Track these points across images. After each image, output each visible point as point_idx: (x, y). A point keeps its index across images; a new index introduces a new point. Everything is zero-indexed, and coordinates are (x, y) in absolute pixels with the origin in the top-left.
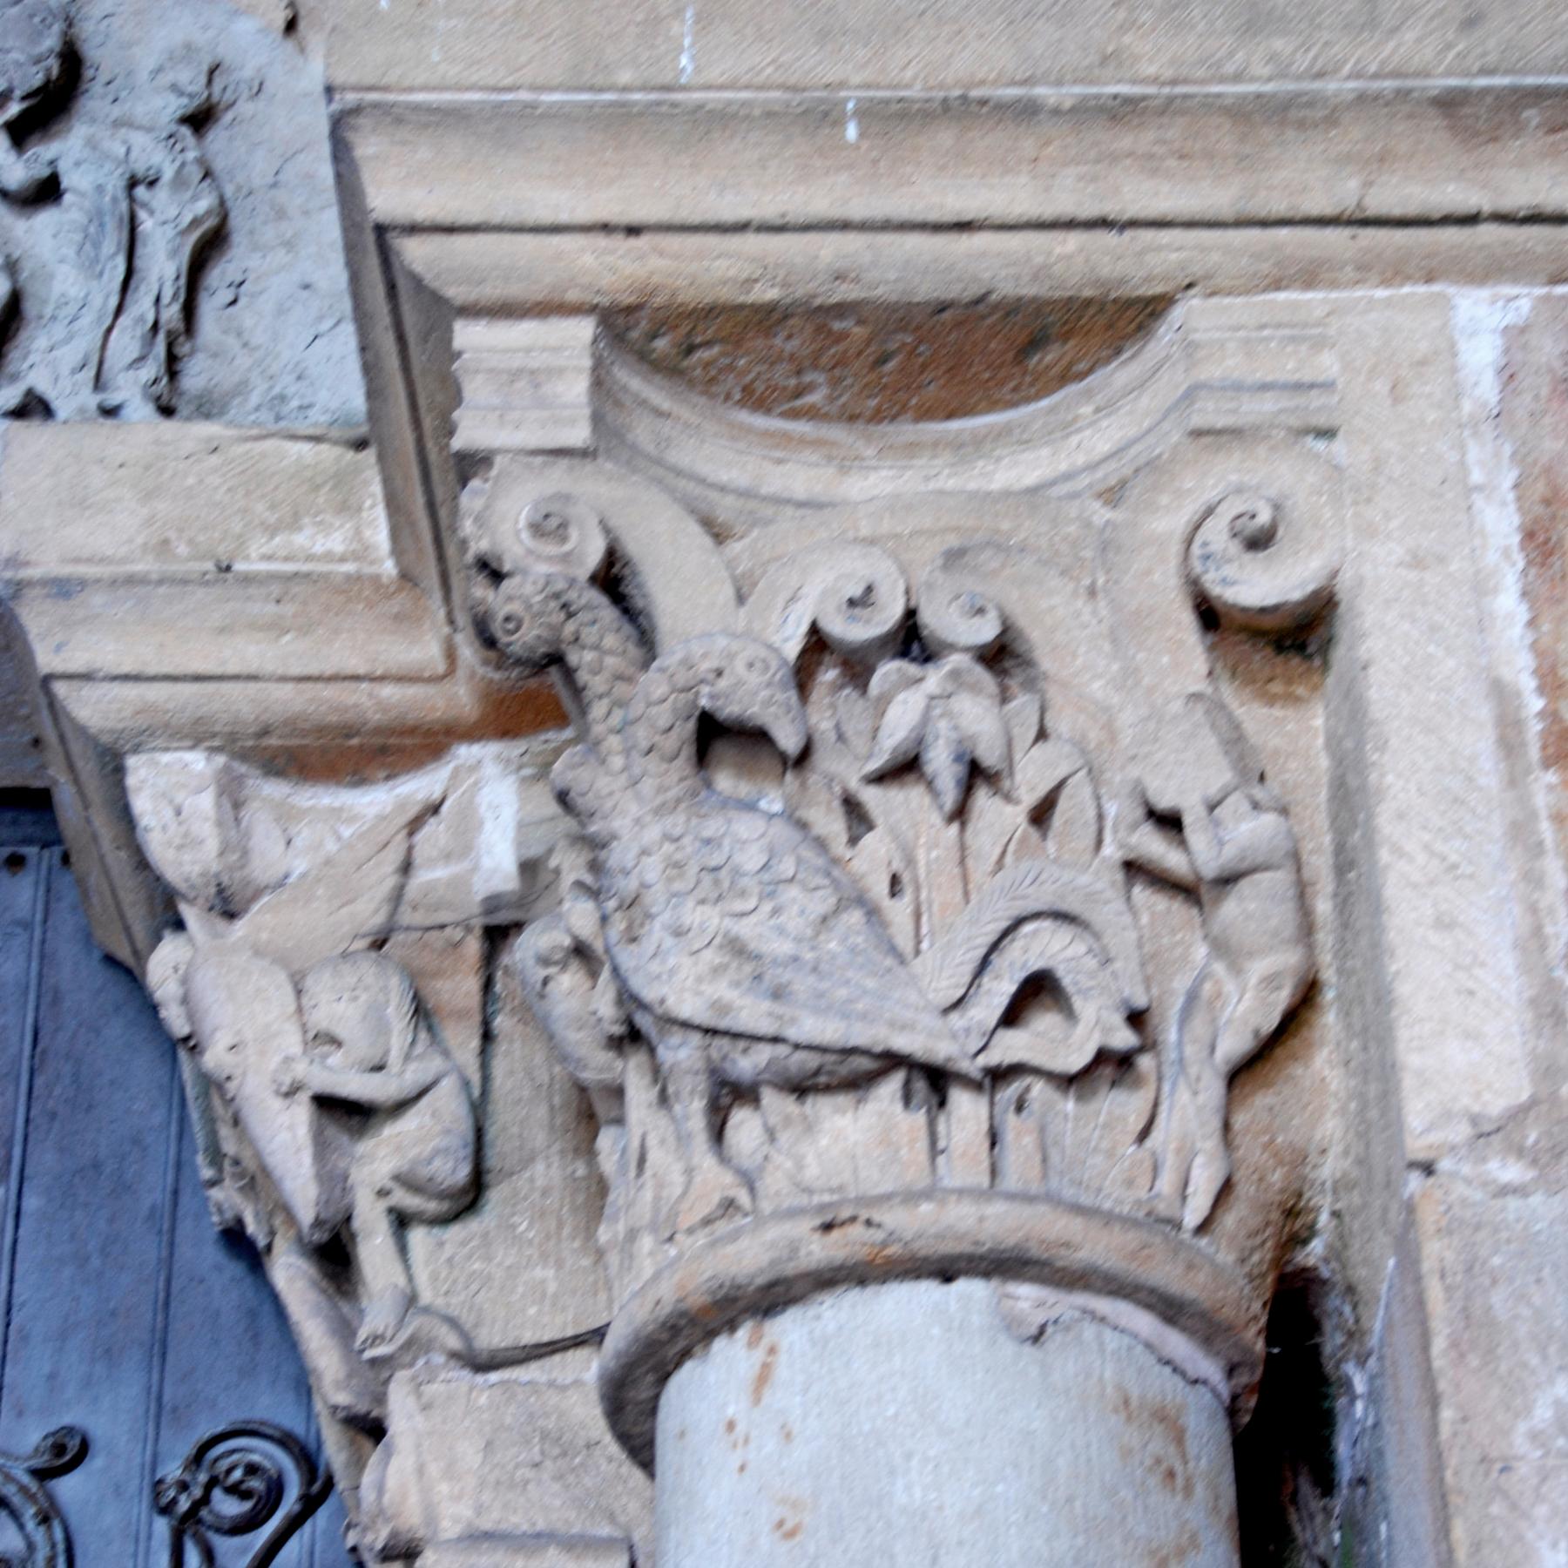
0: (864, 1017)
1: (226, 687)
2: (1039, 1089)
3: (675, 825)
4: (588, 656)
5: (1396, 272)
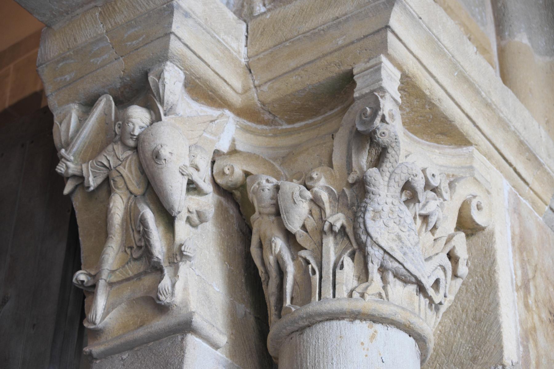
0: (418, 270)
1: (202, 63)
4: (394, 152)
5: (499, 168)
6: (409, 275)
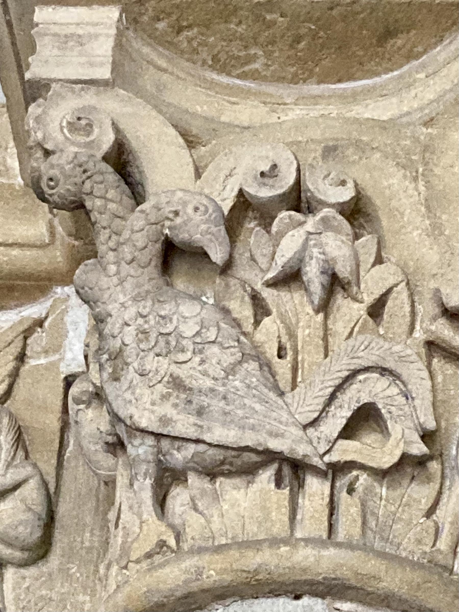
2: (364, 479)
3: (144, 307)
4: (98, 202)
6: (234, 453)
